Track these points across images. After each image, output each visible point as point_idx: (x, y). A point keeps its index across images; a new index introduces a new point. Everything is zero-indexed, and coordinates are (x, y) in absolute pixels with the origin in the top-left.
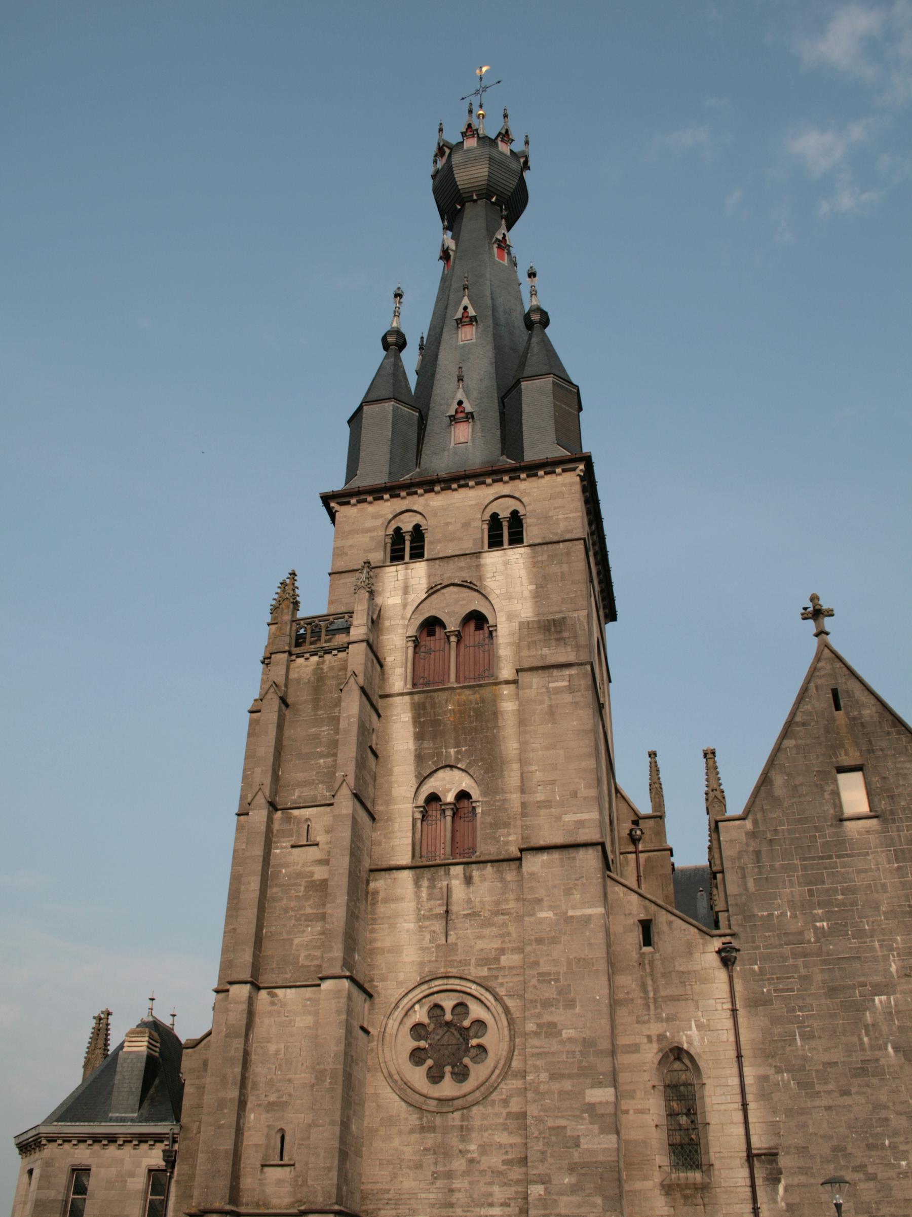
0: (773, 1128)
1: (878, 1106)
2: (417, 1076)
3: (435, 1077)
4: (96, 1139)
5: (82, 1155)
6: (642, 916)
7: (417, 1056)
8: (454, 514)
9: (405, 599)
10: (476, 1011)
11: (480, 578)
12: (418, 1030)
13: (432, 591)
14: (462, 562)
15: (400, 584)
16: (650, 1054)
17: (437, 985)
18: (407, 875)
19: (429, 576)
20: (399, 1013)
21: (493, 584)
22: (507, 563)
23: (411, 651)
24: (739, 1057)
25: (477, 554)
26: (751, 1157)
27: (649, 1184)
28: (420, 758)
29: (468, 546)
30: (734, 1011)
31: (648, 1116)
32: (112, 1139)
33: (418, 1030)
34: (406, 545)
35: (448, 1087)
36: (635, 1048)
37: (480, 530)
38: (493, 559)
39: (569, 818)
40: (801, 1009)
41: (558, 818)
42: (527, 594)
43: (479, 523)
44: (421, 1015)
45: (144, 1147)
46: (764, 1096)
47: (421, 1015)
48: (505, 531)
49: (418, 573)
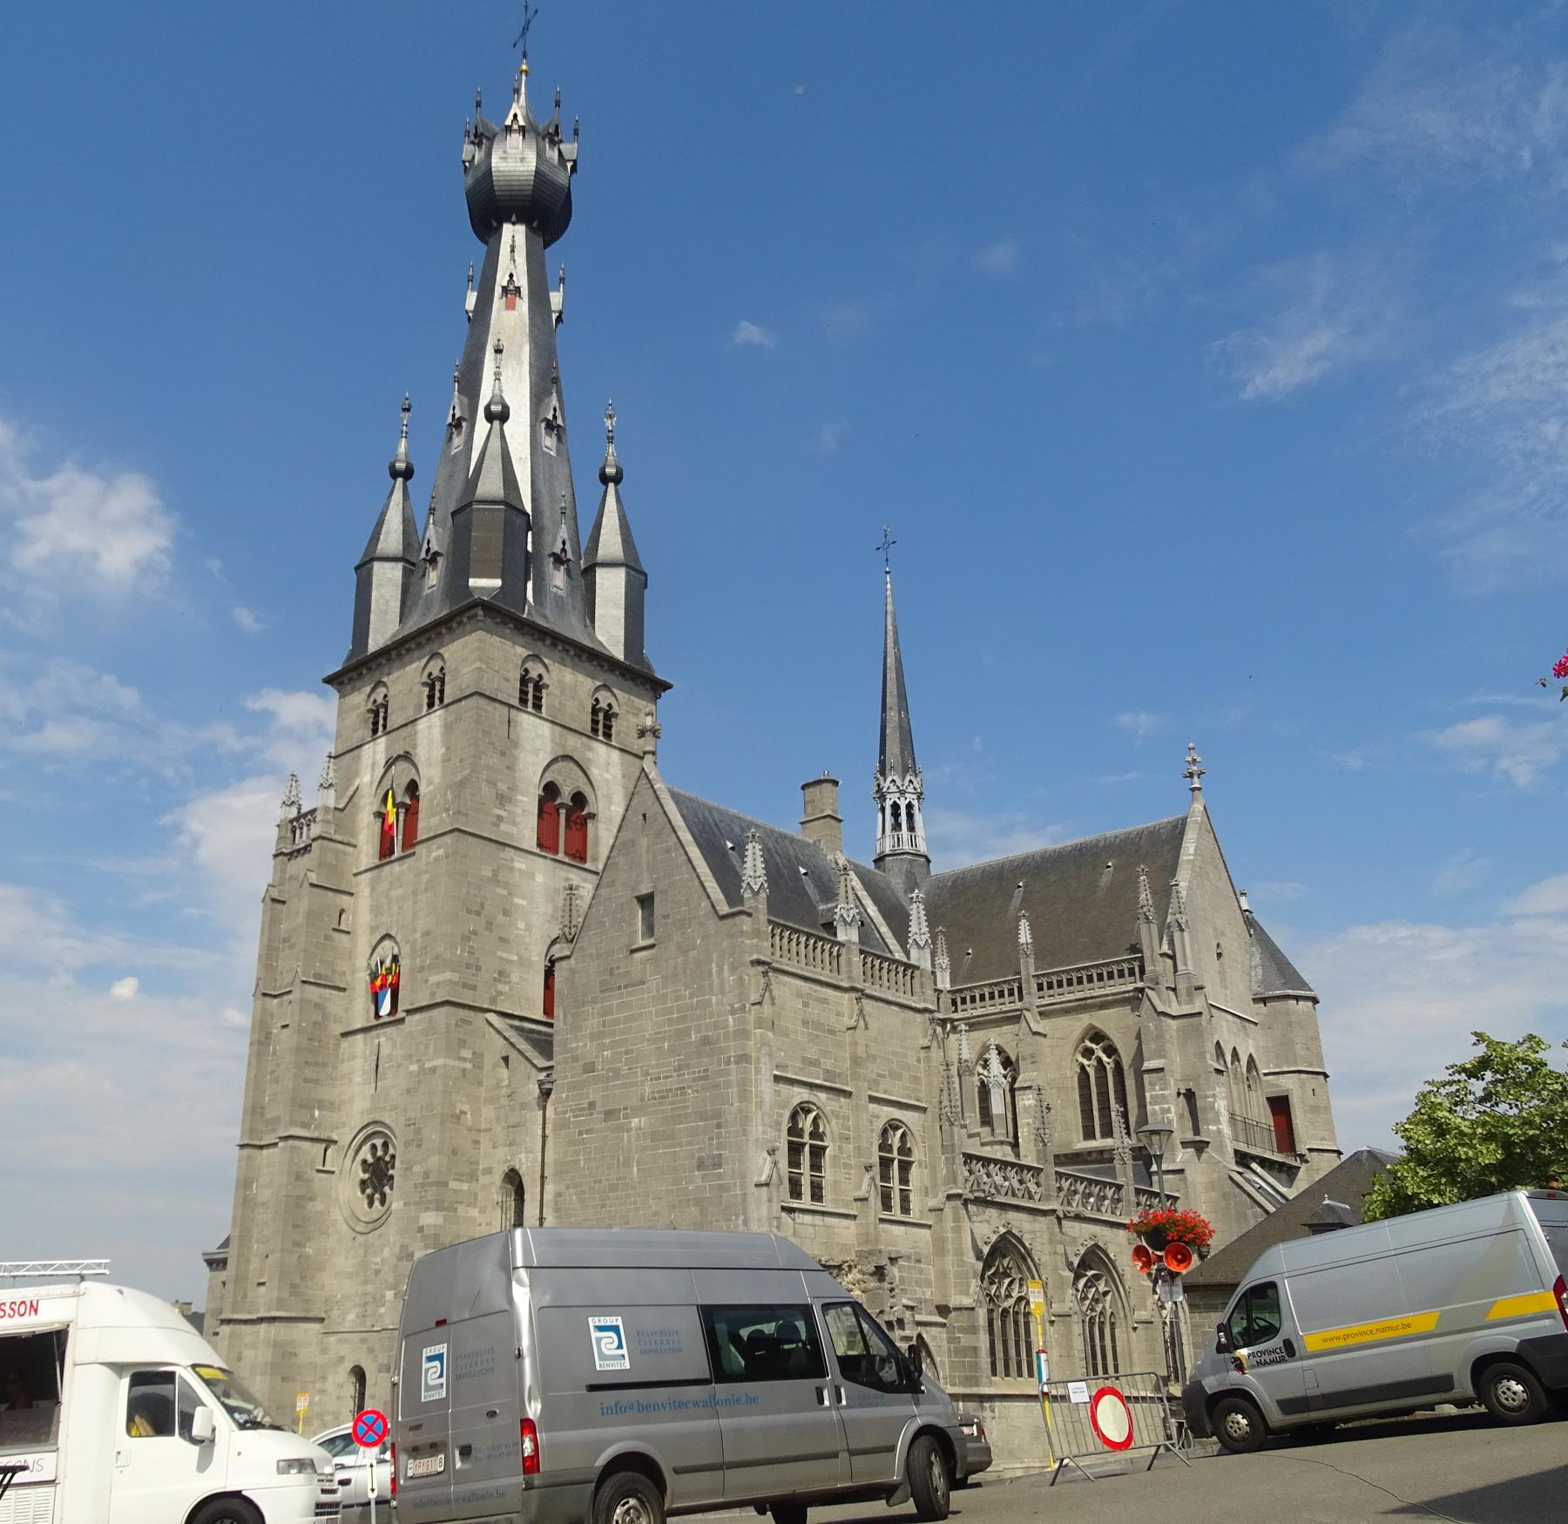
11: (415, 746)
13: (389, 764)
16: (498, 1177)
17: (370, 1130)
19: (387, 749)
20: (351, 1153)
21: (421, 755)
24: (542, 1177)
28: (373, 929)
30: (544, 1137)
34: (378, 720)
39: (433, 979)
40: (587, 1132)
43: (418, 688)
46: (557, 1210)
49: (377, 751)
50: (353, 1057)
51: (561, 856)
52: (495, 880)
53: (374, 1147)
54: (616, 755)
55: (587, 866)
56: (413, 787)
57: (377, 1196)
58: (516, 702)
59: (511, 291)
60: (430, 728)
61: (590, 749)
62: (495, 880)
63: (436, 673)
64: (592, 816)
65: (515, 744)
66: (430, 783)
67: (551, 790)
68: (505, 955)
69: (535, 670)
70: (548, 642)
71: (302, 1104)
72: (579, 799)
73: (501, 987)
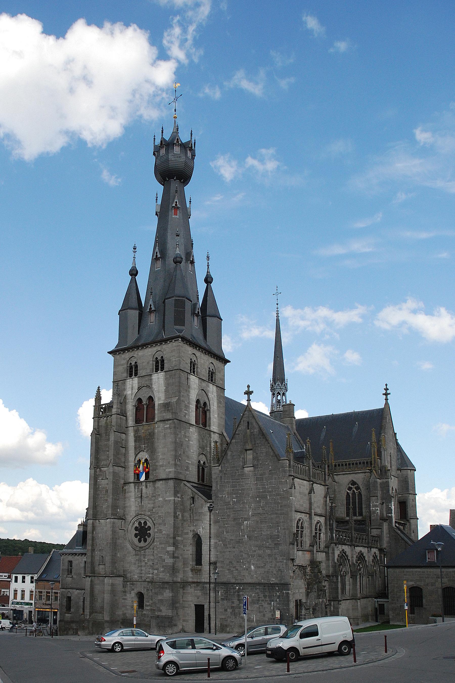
0: (217, 556)
1: (241, 552)
2: (136, 540)
3: (140, 541)
4: (72, 554)
5: (70, 558)
6: (192, 496)
7: (136, 536)
8: (145, 357)
9: (132, 392)
10: (149, 524)
11: (152, 385)
12: (136, 529)
13: (139, 389)
14: (147, 378)
15: (131, 386)
16: (191, 535)
18: (132, 484)
20: (131, 524)
21: (155, 387)
22: (158, 378)
23: (135, 410)
24: (210, 537)
25: (151, 375)
26: (210, 563)
27: (188, 569)
29: (148, 371)
30: (210, 524)
31: (189, 551)
32: (76, 554)
33: (136, 529)
34: (133, 370)
35: (142, 544)
36: (187, 533)
37: (152, 364)
38: (155, 377)
41: (165, 470)
42: (163, 390)
44: (136, 524)
45: (83, 556)
46: (216, 548)
47: (136, 524)
48: (159, 365)
50: (131, 492)
51: (201, 426)
52: (185, 437)
53: (140, 523)
54: (215, 388)
55: (207, 428)
56: (151, 399)
57: (142, 539)
58: (189, 372)
59: (176, 208)
60: (158, 378)
61: (208, 386)
62: (185, 437)
63: (159, 358)
64: (208, 410)
65: (189, 387)
66: (159, 399)
67: (198, 401)
68: (188, 462)
69: (194, 359)
70: (198, 349)
71: (115, 507)
72: (205, 404)
73: (187, 472)
